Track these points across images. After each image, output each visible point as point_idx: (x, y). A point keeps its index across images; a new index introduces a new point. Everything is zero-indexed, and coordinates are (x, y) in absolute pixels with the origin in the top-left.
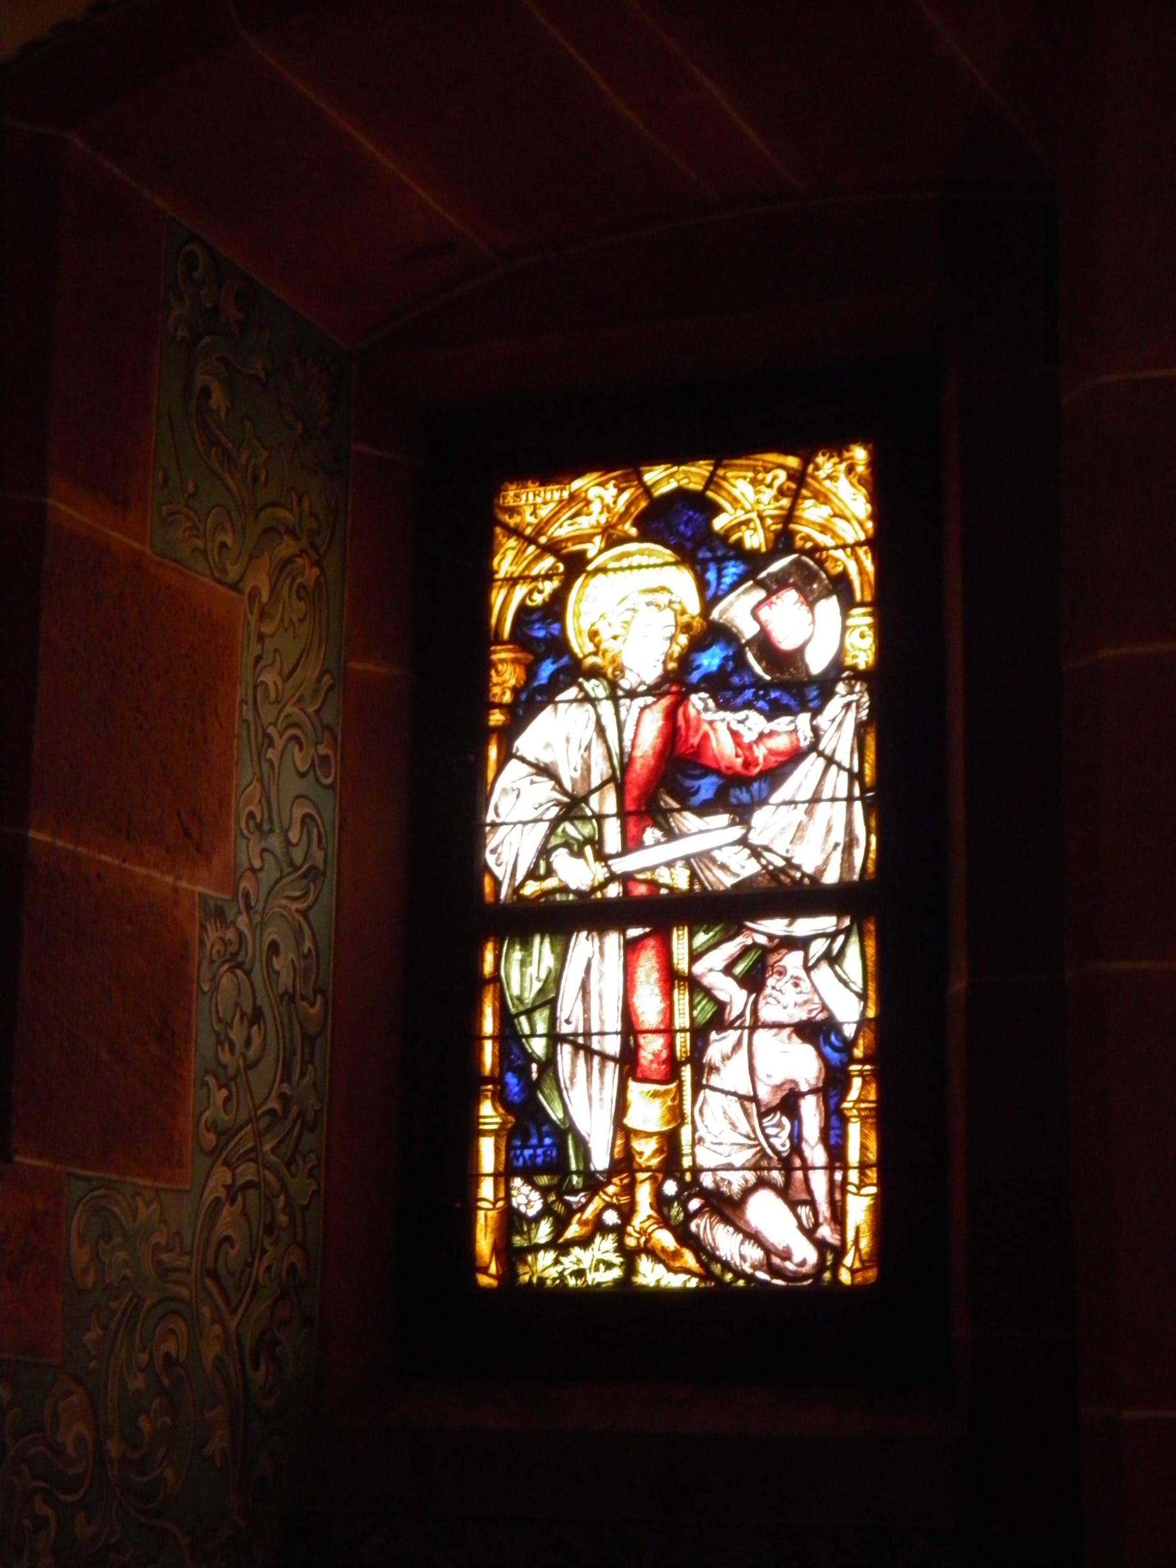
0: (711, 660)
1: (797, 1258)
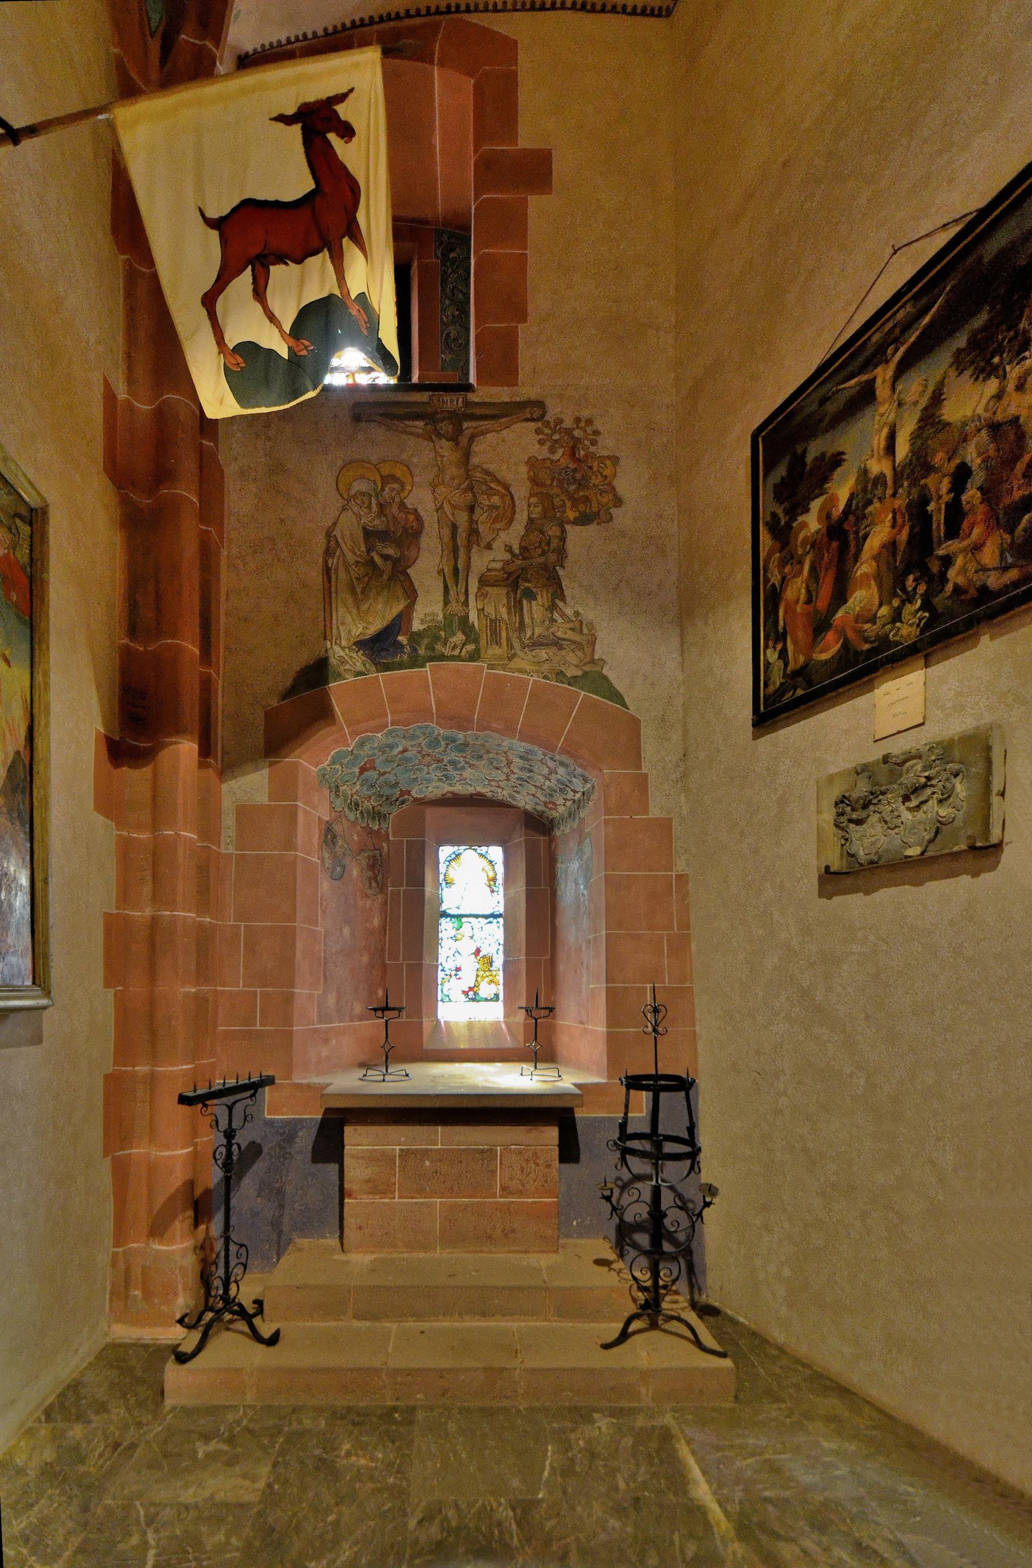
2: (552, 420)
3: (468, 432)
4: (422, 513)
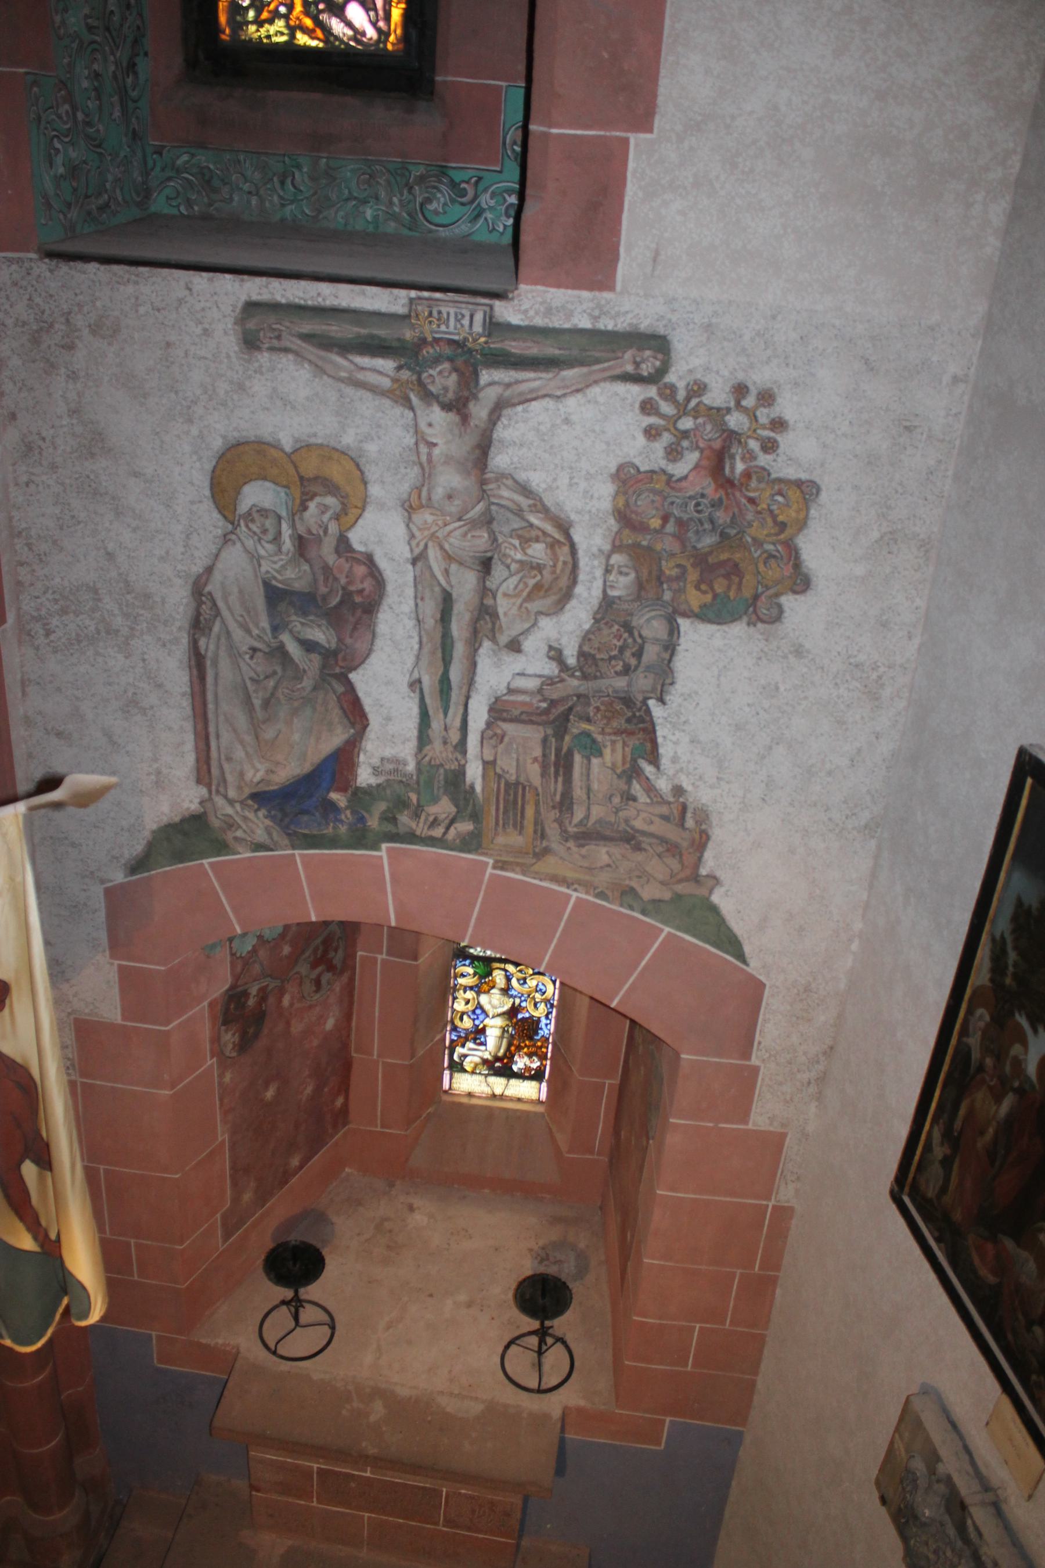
1: (369, 36)
2: (681, 385)
3: (489, 396)
4: (382, 563)
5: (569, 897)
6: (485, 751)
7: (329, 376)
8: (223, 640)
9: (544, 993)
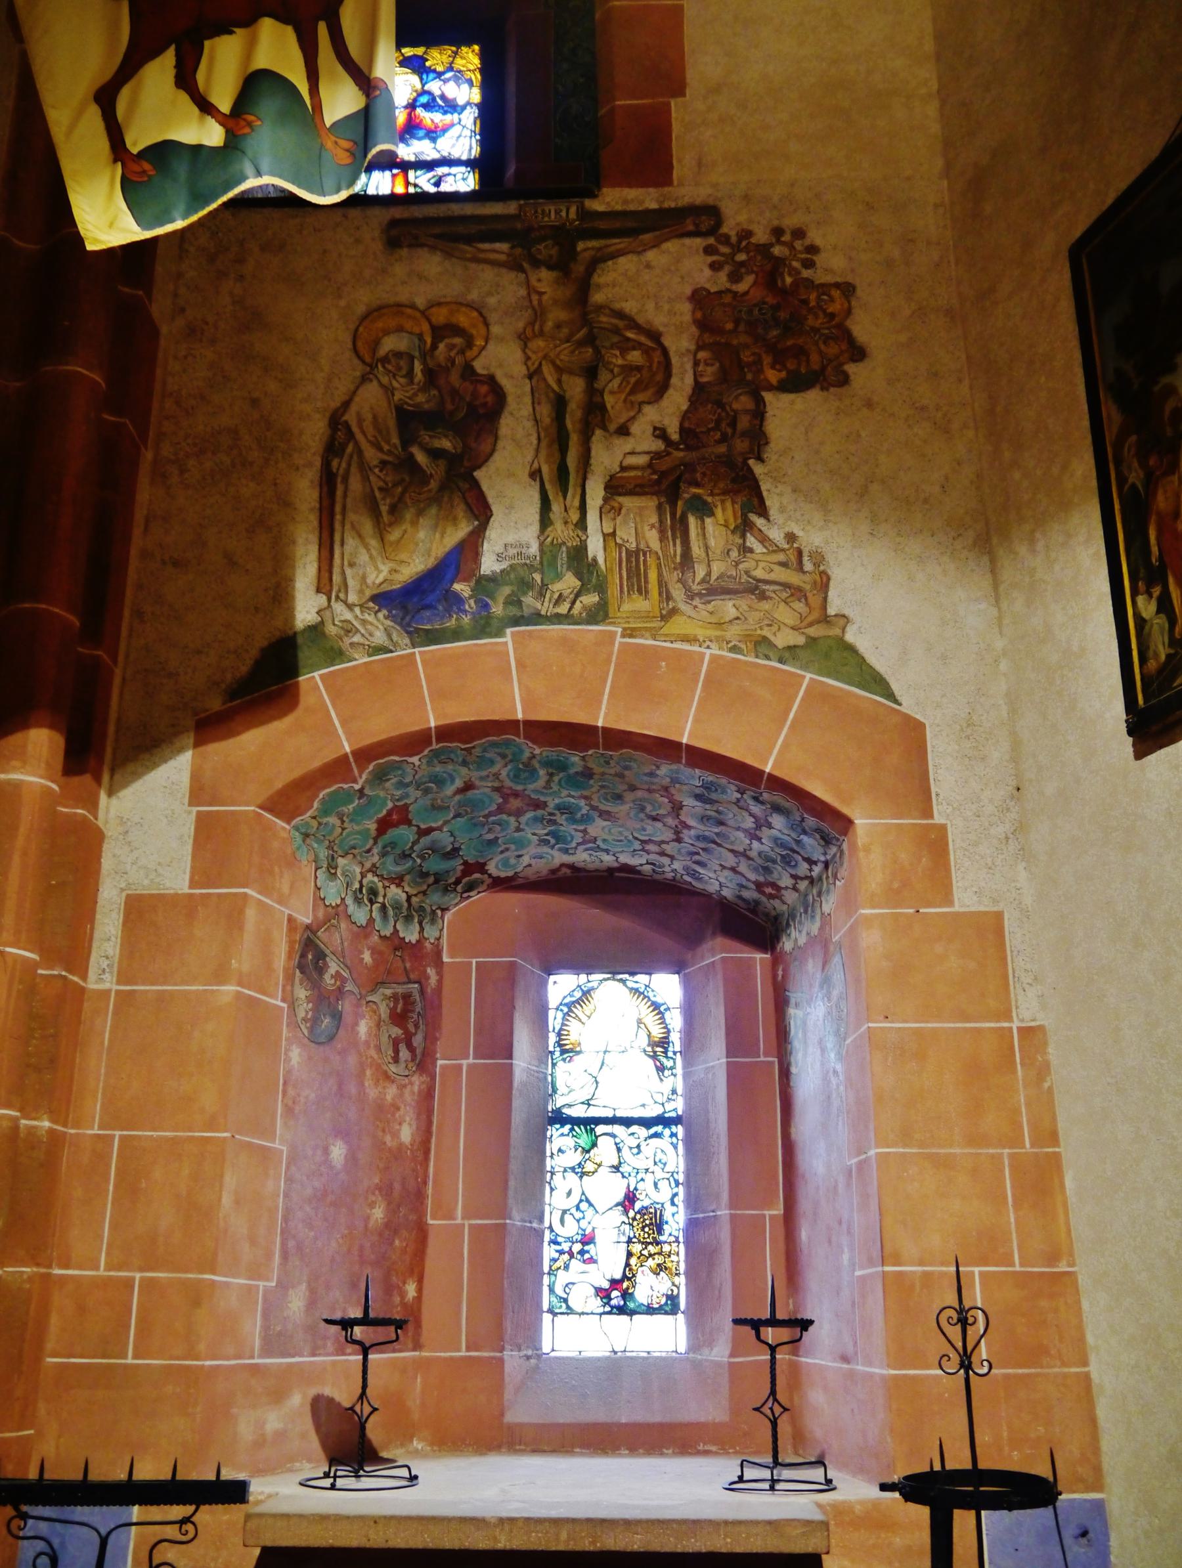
0: (424, 99)
2: (733, 234)
5: (703, 655)
6: (604, 524)
7: (458, 258)
8: (355, 457)
9: (665, 1164)
